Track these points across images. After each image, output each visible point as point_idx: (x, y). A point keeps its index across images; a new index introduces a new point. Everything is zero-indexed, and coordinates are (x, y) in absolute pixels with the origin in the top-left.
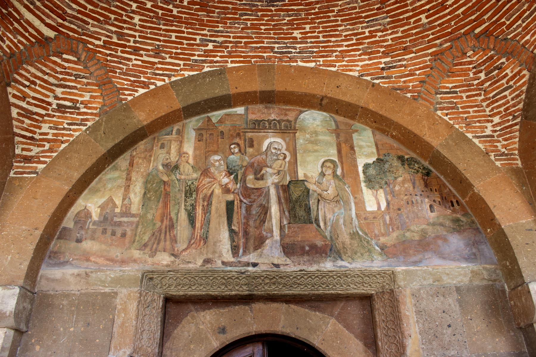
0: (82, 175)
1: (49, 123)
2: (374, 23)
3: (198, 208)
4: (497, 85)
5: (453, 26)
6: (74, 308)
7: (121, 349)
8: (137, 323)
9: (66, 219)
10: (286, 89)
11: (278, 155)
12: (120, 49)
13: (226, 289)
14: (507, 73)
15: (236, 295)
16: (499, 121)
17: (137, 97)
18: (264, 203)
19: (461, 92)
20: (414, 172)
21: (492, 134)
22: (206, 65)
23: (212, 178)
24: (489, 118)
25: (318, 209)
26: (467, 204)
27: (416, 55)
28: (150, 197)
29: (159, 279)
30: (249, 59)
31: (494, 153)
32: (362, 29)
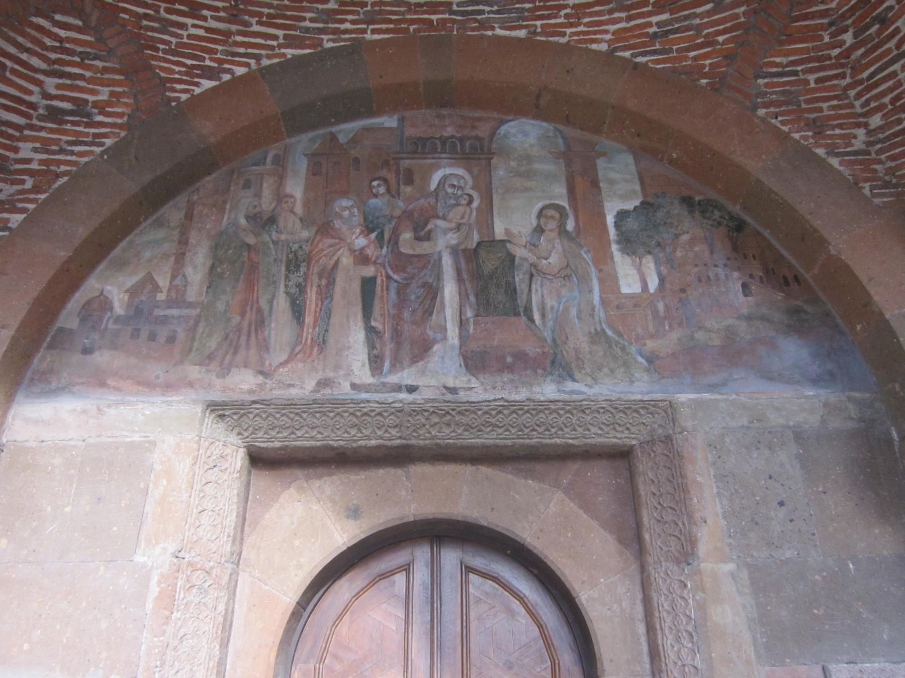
3: (309, 291)
6: (73, 471)
9: (64, 312)
10: (472, 77)
11: (457, 197)
13: (360, 435)
15: (378, 447)
18: (430, 280)
19: (805, 72)
20: (712, 225)
21: (865, 148)
23: (335, 239)
24: (861, 120)
25: (530, 290)
28: (223, 273)
30: (406, 26)
31: (869, 184)
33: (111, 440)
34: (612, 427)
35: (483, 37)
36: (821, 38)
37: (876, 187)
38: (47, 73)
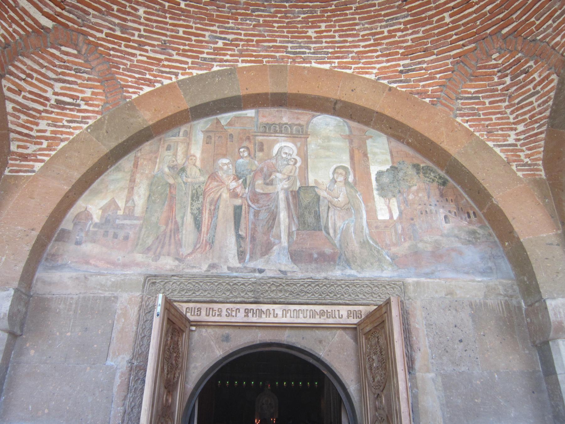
0: (83, 176)
1: (47, 120)
2: (394, 21)
3: (204, 213)
4: (523, 90)
5: (478, 25)
7: (119, 354)
8: (137, 329)
10: (298, 91)
11: (288, 160)
12: (123, 43)
13: (232, 295)
14: (534, 78)
16: (524, 129)
17: (143, 95)
19: (483, 97)
20: (429, 181)
21: (515, 143)
22: (215, 64)
24: (513, 126)
25: (328, 216)
26: (485, 216)
27: (438, 57)
29: (162, 283)
31: (516, 163)
32: (381, 28)
33: (92, 295)
34: (370, 294)
35: (304, 68)
37: (519, 165)
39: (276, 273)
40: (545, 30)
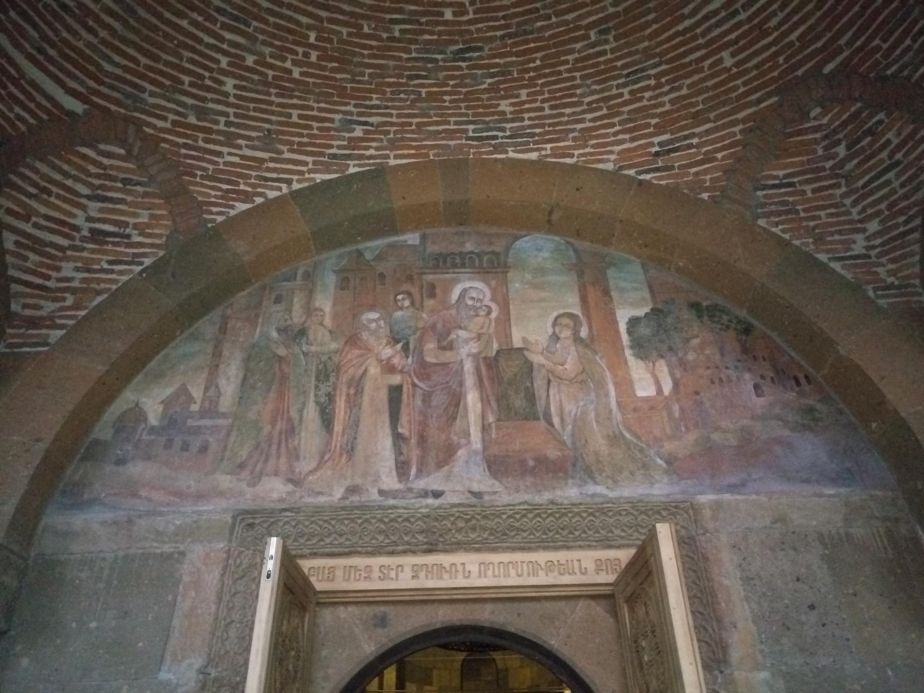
1: (75, 261)
5: (782, 65)
7: (184, 658)
8: (218, 609)
11: (476, 309)
12: (201, 135)
16: (879, 228)
19: (801, 183)
21: (865, 252)
24: (859, 225)
25: (548, 396)
29: (265, 525)
30: (425, 151)
35: (496, 160)
36: (814, 151)
38: (89, 198)
39: (463, 497)
40: (901, 56)
